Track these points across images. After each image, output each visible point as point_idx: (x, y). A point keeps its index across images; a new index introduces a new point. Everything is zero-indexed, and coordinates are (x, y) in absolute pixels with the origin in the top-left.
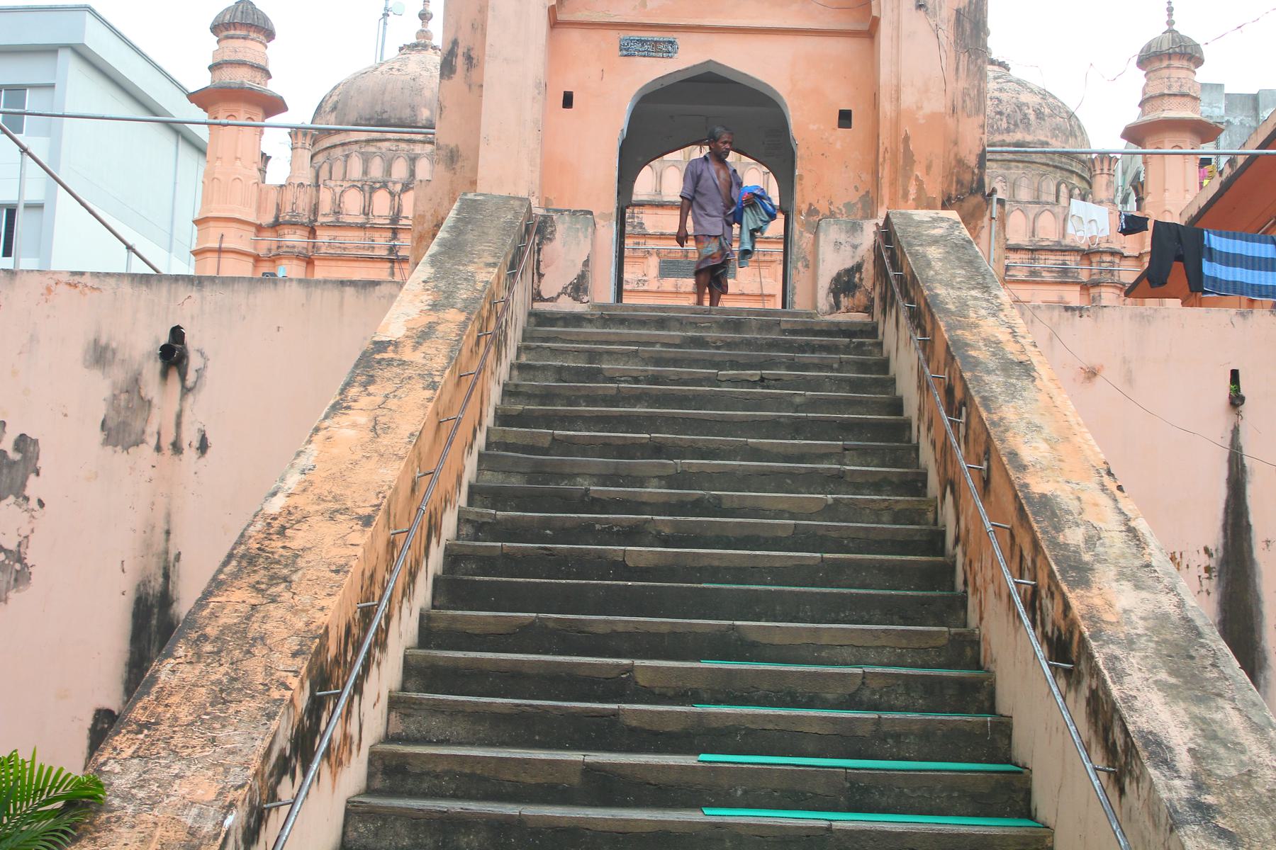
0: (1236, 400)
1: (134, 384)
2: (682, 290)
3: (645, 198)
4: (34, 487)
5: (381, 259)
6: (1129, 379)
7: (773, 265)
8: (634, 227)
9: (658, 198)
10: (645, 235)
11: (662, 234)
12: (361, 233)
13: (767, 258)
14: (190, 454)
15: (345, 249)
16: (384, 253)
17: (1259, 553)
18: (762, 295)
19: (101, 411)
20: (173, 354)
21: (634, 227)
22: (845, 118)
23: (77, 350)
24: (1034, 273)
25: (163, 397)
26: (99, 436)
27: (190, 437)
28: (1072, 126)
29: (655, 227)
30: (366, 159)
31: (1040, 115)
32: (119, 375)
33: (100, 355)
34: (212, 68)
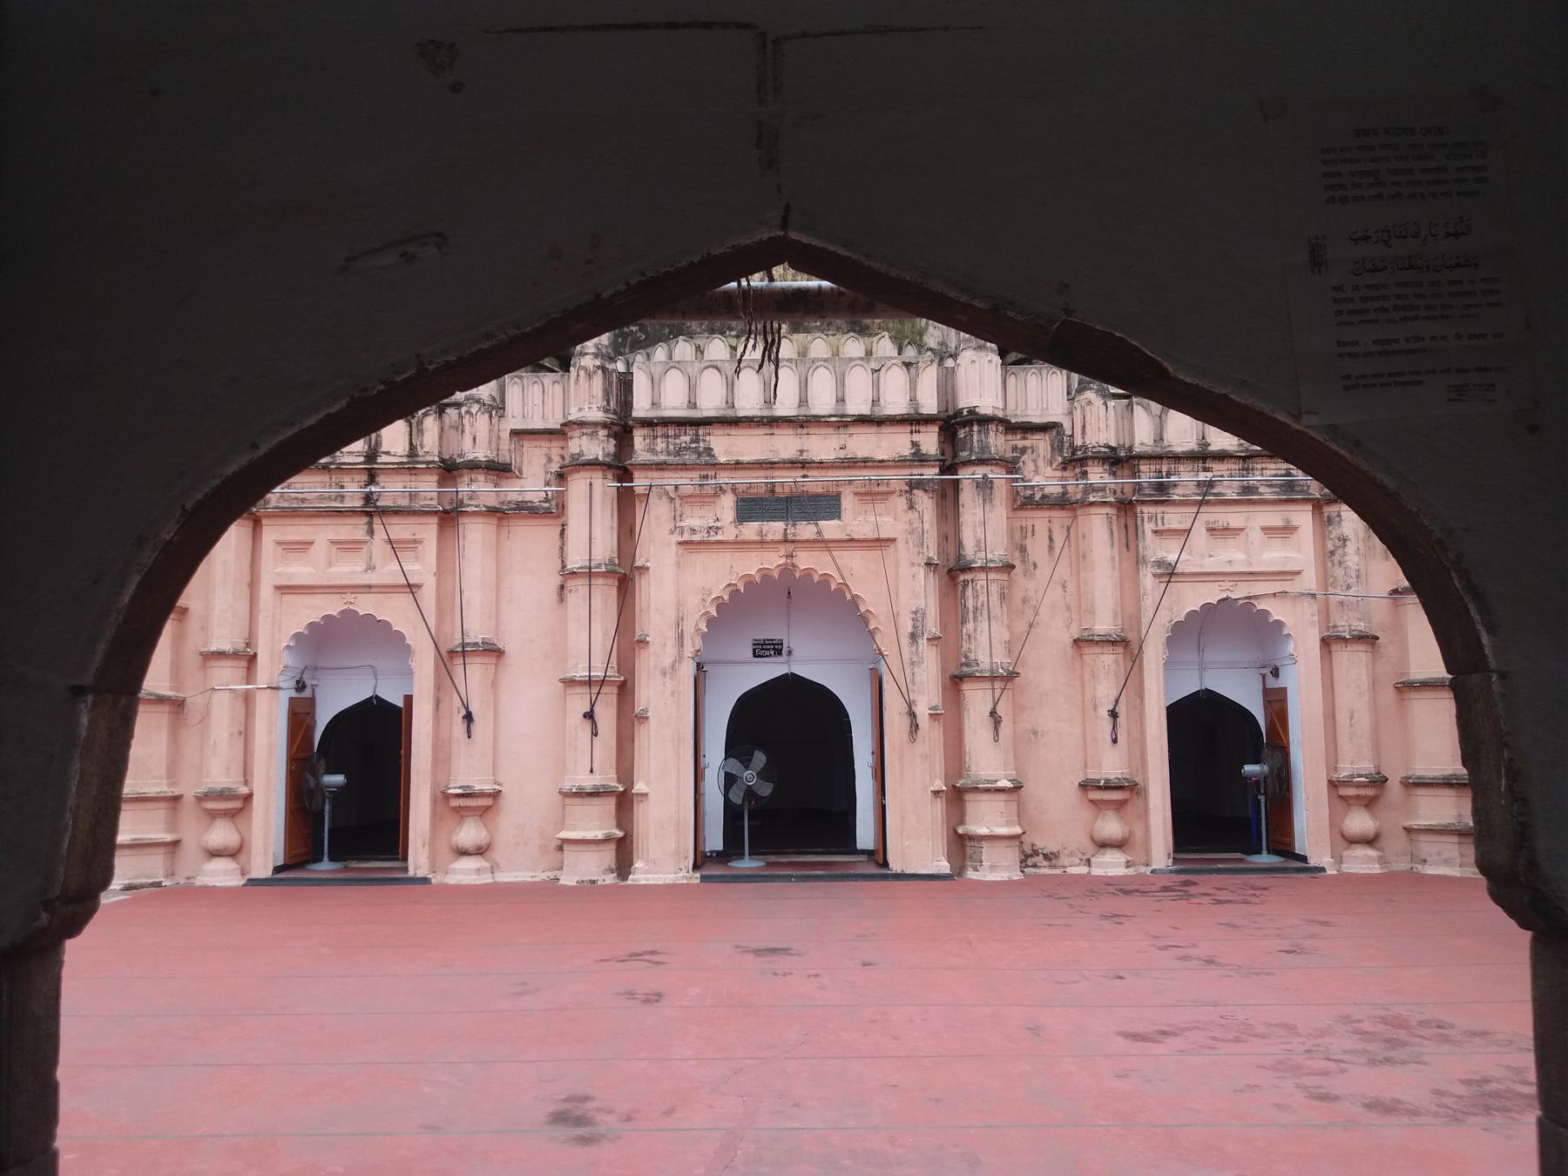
2: (770, 538)
3: (713, 414)
5: (353, 512)
7: (892, 498)
8: (700, 455)
9: (730, 413)
10: (716, 466)
11: (738, 463)
12: (327, 478)
13: (883, 488)
15: (303, 500)
16: (358, 503)
18: (877, 540)
21: (700, 455)
24: (1247, 489)
29: (727, 452)
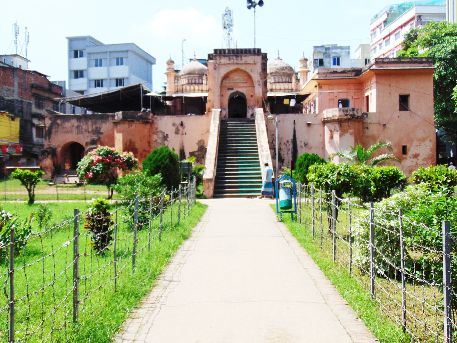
0: (294, 123)
1: (178, 128)
4: (168, 139)
6: (283, 122)
14: (184, 135)
17: (297, 140)
19: (174, 131)
20: (182, 124)
22: (252, 96)
23: (171, 124)
25: (181, 128)
26: (174, 133)
27: (184, 133)
28: (291, 69)
30: (188, 80)
31: (286, 68)
32: (176, 127)
33: (174, 125)
34: (167, 69)
